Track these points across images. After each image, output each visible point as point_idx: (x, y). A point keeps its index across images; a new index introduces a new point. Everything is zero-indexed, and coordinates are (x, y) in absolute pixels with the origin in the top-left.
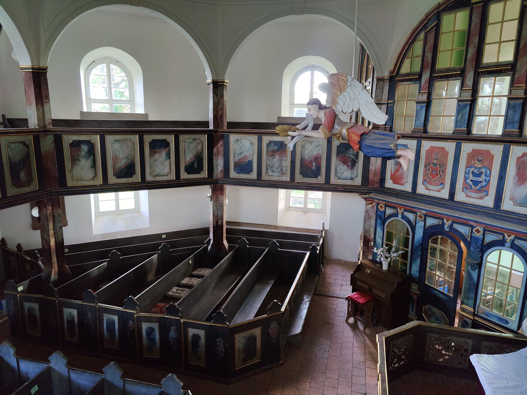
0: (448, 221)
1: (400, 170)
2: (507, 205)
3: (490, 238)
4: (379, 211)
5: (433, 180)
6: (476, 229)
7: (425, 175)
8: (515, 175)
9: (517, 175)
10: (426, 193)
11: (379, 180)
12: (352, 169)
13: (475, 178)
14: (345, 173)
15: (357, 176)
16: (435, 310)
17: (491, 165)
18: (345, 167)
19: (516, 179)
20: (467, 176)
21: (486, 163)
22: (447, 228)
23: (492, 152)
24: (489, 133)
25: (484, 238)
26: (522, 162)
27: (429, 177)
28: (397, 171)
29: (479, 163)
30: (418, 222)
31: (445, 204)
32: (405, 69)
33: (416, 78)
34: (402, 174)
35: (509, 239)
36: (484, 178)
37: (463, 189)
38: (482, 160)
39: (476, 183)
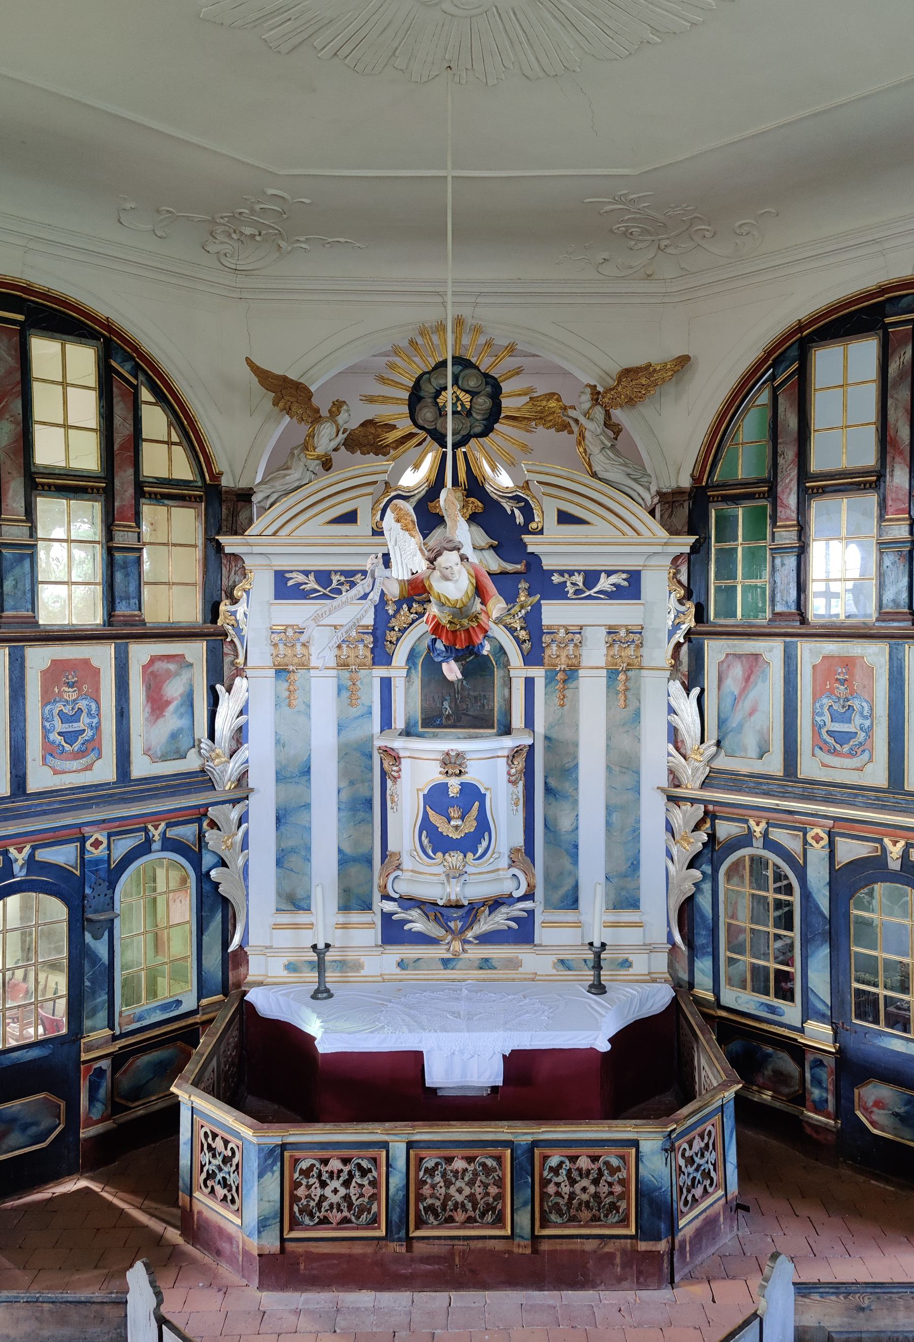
0: (20, 850)
2: (141, 767)
3: (123, 847)
6: (92, 840)
8: (145, 702)
9: (148, 702)
13: (66, 725)
17: (98, 690)
19: (148, 709)
21: (85, 688)
22: (20, 871)
23: (95, 663)
24: (74, 622)
25: (109, 855)
26: (152, 672)
29: (70, 690)
35: (156, 834)
36: (87, 721)
37: (44, 758)
38: (76, 682)
39: (70, 737)
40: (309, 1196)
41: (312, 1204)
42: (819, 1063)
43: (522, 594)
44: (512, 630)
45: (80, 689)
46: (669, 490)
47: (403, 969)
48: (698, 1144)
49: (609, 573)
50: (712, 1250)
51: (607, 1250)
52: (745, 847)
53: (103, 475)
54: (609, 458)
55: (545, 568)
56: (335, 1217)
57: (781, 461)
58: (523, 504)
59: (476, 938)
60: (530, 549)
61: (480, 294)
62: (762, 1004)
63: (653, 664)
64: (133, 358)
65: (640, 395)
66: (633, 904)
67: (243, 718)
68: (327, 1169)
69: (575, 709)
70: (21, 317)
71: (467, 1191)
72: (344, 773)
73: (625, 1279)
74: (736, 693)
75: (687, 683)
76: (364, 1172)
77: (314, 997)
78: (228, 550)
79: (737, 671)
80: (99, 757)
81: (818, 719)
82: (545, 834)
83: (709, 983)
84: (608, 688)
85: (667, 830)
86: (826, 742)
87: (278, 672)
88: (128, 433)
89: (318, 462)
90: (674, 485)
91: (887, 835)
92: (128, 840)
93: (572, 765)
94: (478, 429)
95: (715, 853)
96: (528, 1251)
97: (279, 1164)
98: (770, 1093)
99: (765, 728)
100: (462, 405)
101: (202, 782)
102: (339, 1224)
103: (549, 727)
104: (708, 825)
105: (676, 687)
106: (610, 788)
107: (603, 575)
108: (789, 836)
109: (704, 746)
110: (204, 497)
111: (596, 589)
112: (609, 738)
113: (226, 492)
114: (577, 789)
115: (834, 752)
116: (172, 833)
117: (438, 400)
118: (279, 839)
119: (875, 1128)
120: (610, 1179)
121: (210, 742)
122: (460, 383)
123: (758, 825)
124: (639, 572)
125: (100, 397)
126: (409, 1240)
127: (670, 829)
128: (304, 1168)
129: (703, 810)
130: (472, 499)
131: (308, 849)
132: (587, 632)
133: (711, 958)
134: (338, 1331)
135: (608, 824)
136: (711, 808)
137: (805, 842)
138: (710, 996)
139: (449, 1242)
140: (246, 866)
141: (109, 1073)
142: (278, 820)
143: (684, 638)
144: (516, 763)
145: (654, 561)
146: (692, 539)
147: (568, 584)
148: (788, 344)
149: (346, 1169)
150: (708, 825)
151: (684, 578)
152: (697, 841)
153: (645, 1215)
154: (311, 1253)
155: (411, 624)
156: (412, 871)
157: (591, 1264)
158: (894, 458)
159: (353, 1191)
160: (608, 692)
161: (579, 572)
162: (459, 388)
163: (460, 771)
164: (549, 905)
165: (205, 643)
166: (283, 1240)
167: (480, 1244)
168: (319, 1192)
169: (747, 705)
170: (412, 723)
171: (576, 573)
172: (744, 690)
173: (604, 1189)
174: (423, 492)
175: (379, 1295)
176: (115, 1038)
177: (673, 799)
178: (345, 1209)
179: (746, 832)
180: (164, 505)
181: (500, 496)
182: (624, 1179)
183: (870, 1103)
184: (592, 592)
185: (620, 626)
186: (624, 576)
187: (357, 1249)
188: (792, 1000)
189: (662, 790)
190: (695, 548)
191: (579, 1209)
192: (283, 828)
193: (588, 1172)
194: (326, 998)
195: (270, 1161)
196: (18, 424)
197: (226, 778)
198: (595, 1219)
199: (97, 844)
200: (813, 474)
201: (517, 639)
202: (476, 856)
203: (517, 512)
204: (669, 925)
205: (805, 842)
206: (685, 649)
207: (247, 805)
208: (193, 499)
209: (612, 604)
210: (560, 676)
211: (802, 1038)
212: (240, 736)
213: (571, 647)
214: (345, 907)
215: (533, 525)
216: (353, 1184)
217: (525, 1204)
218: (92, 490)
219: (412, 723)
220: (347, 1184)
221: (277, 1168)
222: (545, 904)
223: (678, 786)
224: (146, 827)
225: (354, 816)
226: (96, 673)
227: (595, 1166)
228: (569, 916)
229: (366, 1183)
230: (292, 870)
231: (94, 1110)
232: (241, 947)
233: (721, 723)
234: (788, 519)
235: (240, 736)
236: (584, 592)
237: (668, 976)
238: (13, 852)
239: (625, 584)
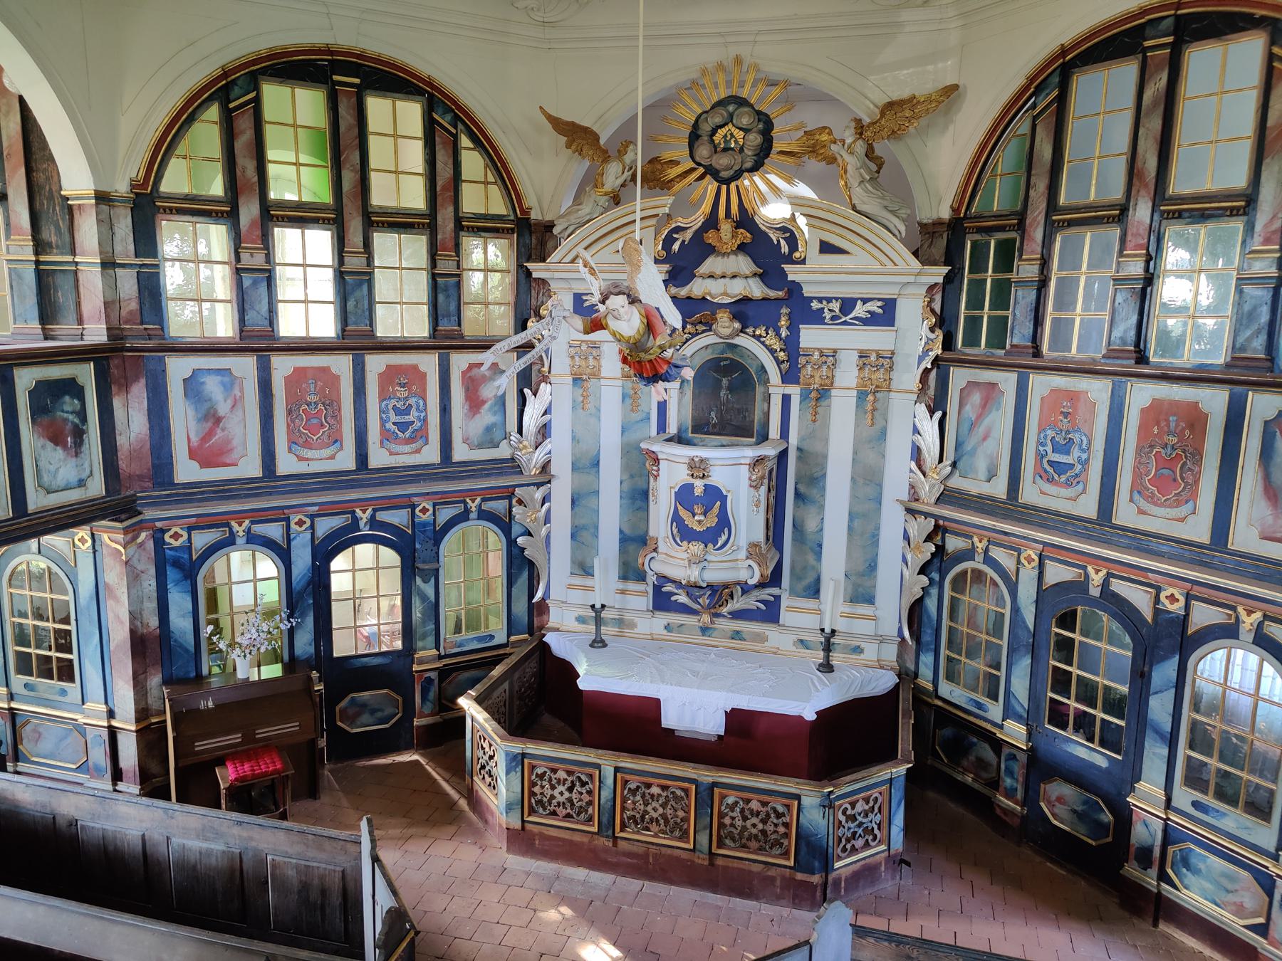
0: (364, 512)
1: (219, 431)
2: (461, 453)
3: (445, 514)
4: (168, 548)
5: (315, 438)
6: (421, 507)
7: (290, 432)
10: (302, 468)
11: (149, 470)
12: (77, 455)
14: (61, 471)
15: (91, 471)
16: (365, 695)
17: (424, 390)
18: (60, 452)
19: (467, 407)
20: (384, 416)
23: (422, 368)
24: (406, 335)
25: (435, 520)
27: (303, 433)
28: (210, 434)
30: (294, 538)
31: (353, 480)
32: (175, 180)
33: (222, 212)
34: (229, 441)
35: (473, 506)
36: (416, 414)
37: (382, 442)
38: (406, 383)
39: (403, 427)
40: (542, 794)
41: (545, 799)
42: (1012, 757)
43: (783, 318)
44: (772, 351)
45: (410, 389)
46: (930, 221)
47: (669, 632)
48: (860, 806)
49: (865, 301)
50: (869, 891)
51: (769, 873)
53: (428, 212)
54: (867, 191)
55: (805, 295)
56: (562, 812)
57: (1032, 193)
58: (788, 235)
59: (729, 613)
60: (790, 278)
61: (759, 32)
63: (902, 387)
64: (453, 110)
65: (903, 127)
66: (870, 600)
67: (547, 417)
68: (555, 776)
69: (826, 426)
70: (357, 81)
71: (661, 810)
72: (626, 467)
73: (784, 899)
76: (583, 784)
77: (591, 646)
78: (535, 275)
79: (976, 398)
80: (427, 443)
81: (1041, 449)
82: (793, 532)
83: (930, 675)
84: (857, 407)
86: (1046, 471)
87: (574, 380)
88: (449, 176)
89: (607, 197)
90: (935, 216)
91: (1090, 564)
92: (450, 509)
93: (820, 474)
94: (748, 165)
95: (943, 564)
96: (706, 863)
97: (520, 767)
98: (972, 775)
100: (736, 142)
101: (513, 467)
102: (564, 817)
103: (801, 439)
105: (922, 409)
106: (854, 497)
107: (859, 301)
110: (516, 230)
111: (851, 316)
112: (855, 453)
113: (535, 224)
114: (823, 496)
115: (1050, 480)
116: (486, 506)
117: (714, 138)
118: (573, 516)
119: (1055, 819)
120: (775, 821)
121: (518, 436)
122: (734, 122)
123: (980, 542)
124: (895, 300)
125: (426, 145)
126: (615, 839)
127: (906, 537)
128: (539, 773)
129: (933, 524)
130: (742, 230)
131: (597, 528)
132: (841, 355)
134: (552, 892)
135: (850, 529)
136: (941, 522)
137: (1019, 562)
138: (930, 687)
139: (645, 845)
140: (548, 537)
141: (436, 682)
142: (573, 502)
143: (932, 364)
144: (756, 470)
145: (910, 290)
146: (945, 270)
147: (826, 310)
148: (1050, 70)
149: (570, 779)
150: (939, 538)
151: (937, 307)
153: (802, 853)
154: (543, 834)
155: (685, 343)
156: (666, 554)
157: (755, 882)
158: (1139, 191)
159: (574, 796)
160: (857, 411)
161: (837, 299)
162: (733, 125)
163: (704, 475)
164: (794, 593)
165: (516, 354)
166: (523, 821)
167: (669, 851)
168: (550, 792)
169: (981, 430)
170: (683, 428)
171: (834, 301)
172: (980, 417)
173: (770, 828)
174: (700, 224)
175: (592, 873)
176: (440, 657)
177: (911, 511)
178: (569, 808)
180: (481, 237)
181: (767, 227)
182: (787, 823)
183: (1053, 798)
184: (847, 318)
185: (868, 350)
186: (880, 304)
187: (577, 838)
188: (996, 699)
189: (901, 502)
190: (948, 279)
191: (749, 839)
192: (576, 509)
193: (758, 813)
194: (599, 647)
195: (514, 764)
196: (356, 172)
197: (532, 466)
198: (761, 849)
199: (424, 511)
200: (1061, 207)
201: (776, 359)
202: (717, 547)
203: (783, 242)
204: (900, 621)
205: (1019, 562)
207: (550, 488)
208: (505, 231)
209: (866, 330)
210: (813, 395)
212: (544, 431)
213: (824, 368)
214: (624, 577)
215: (797, 255)
216: (575, 791)
217: (705, 828)
218: (419, 225)
219: (683, 428)
220: (570, 789)
221: (519, 769)
222: (790, 593)
223: (917, 500)
224: (465, 500)
225: (633, 504)
226: (423, 376)
227: (764, 810)
228: (810, 603)
229: (584, 792)
230: (583, 543)
231: (425, 707)
232: (543, 599)
233: (958, 445)
234: (1033, 252)
235: (544, 431)
236: (841, 318)
237: (896, 664)
238: (359, 512)
239: (880, 311)
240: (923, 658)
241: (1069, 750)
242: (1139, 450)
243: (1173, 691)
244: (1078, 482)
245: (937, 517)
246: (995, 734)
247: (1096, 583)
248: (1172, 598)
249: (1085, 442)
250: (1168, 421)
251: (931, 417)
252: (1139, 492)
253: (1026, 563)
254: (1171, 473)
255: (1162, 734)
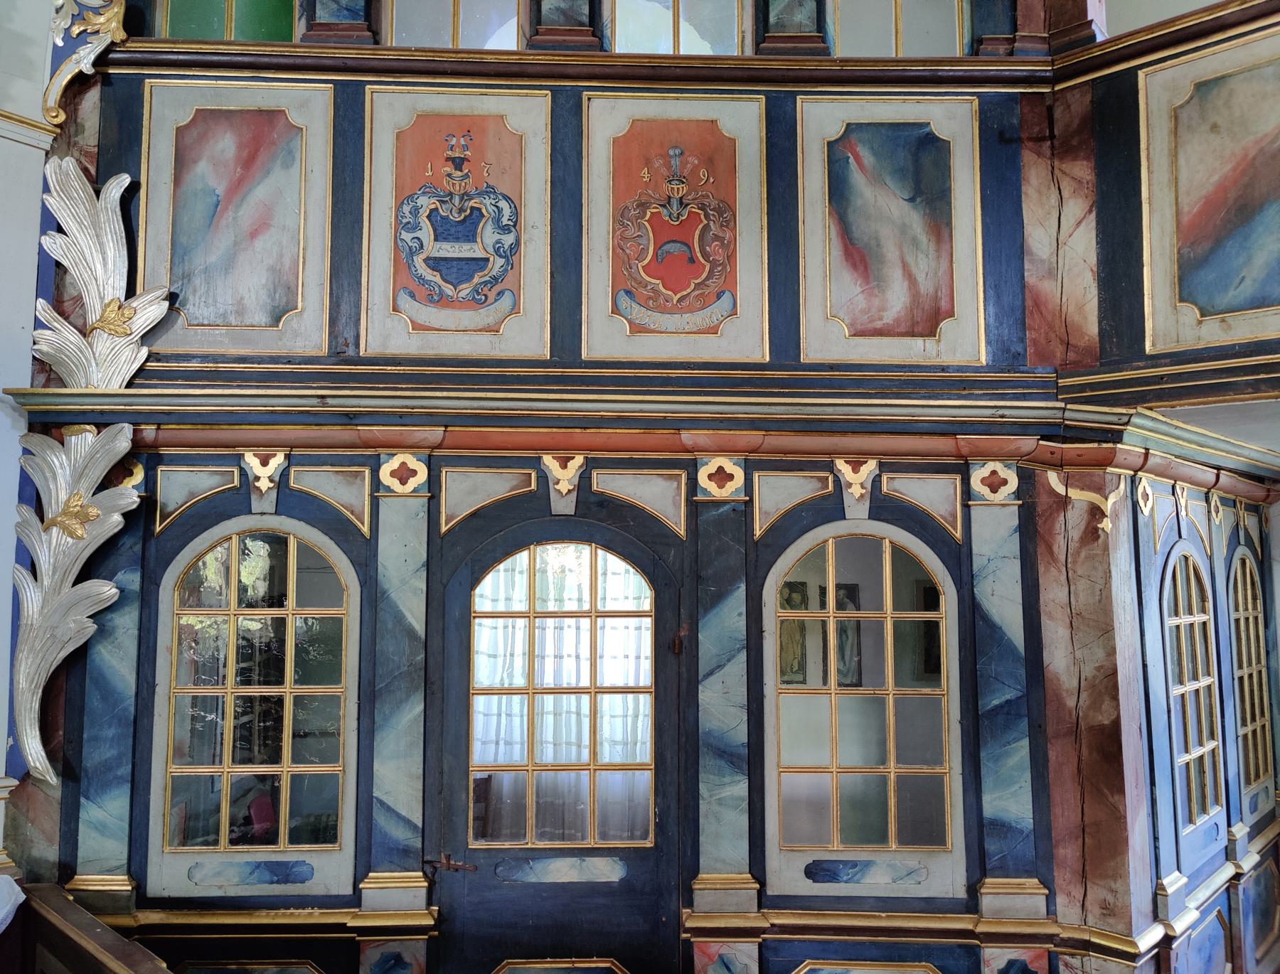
52: (229, 517)
62: (258, 865)
74: (221, 190)
75: (93, 170)
79: (225, 144)
83: (117, 850)
85: (22, 499)
99: (287, 262)
104: (139, 475)
108: (340, 477)
109: (135, 303)
123: (264, 463)
127: (31, 496)
133: (127, 789)
136: (149, 432)
137: (376, 484)
138: (120, 884)
143: (95, 64)
150: (139, 475)
152: (109, 511)
169: (247, 212)
172: (239, 186)
179: (236, 483)
189: (16, 394)
206: (92, 100)
211: (355, 916)
240: (90, 812)
241: (534, 880)
242: (620, 217)
243: (743, 656)
244: (501, 293)
245: (137, 419)
246: (342, 927)
247: (564, 487)
248: (721, 476)
249: (507, 212)
250: (666, 157)
251: (98, 193)
252: (628, 293)
253: (394, 484)
254: (685, 248)
255: (731, 755)
